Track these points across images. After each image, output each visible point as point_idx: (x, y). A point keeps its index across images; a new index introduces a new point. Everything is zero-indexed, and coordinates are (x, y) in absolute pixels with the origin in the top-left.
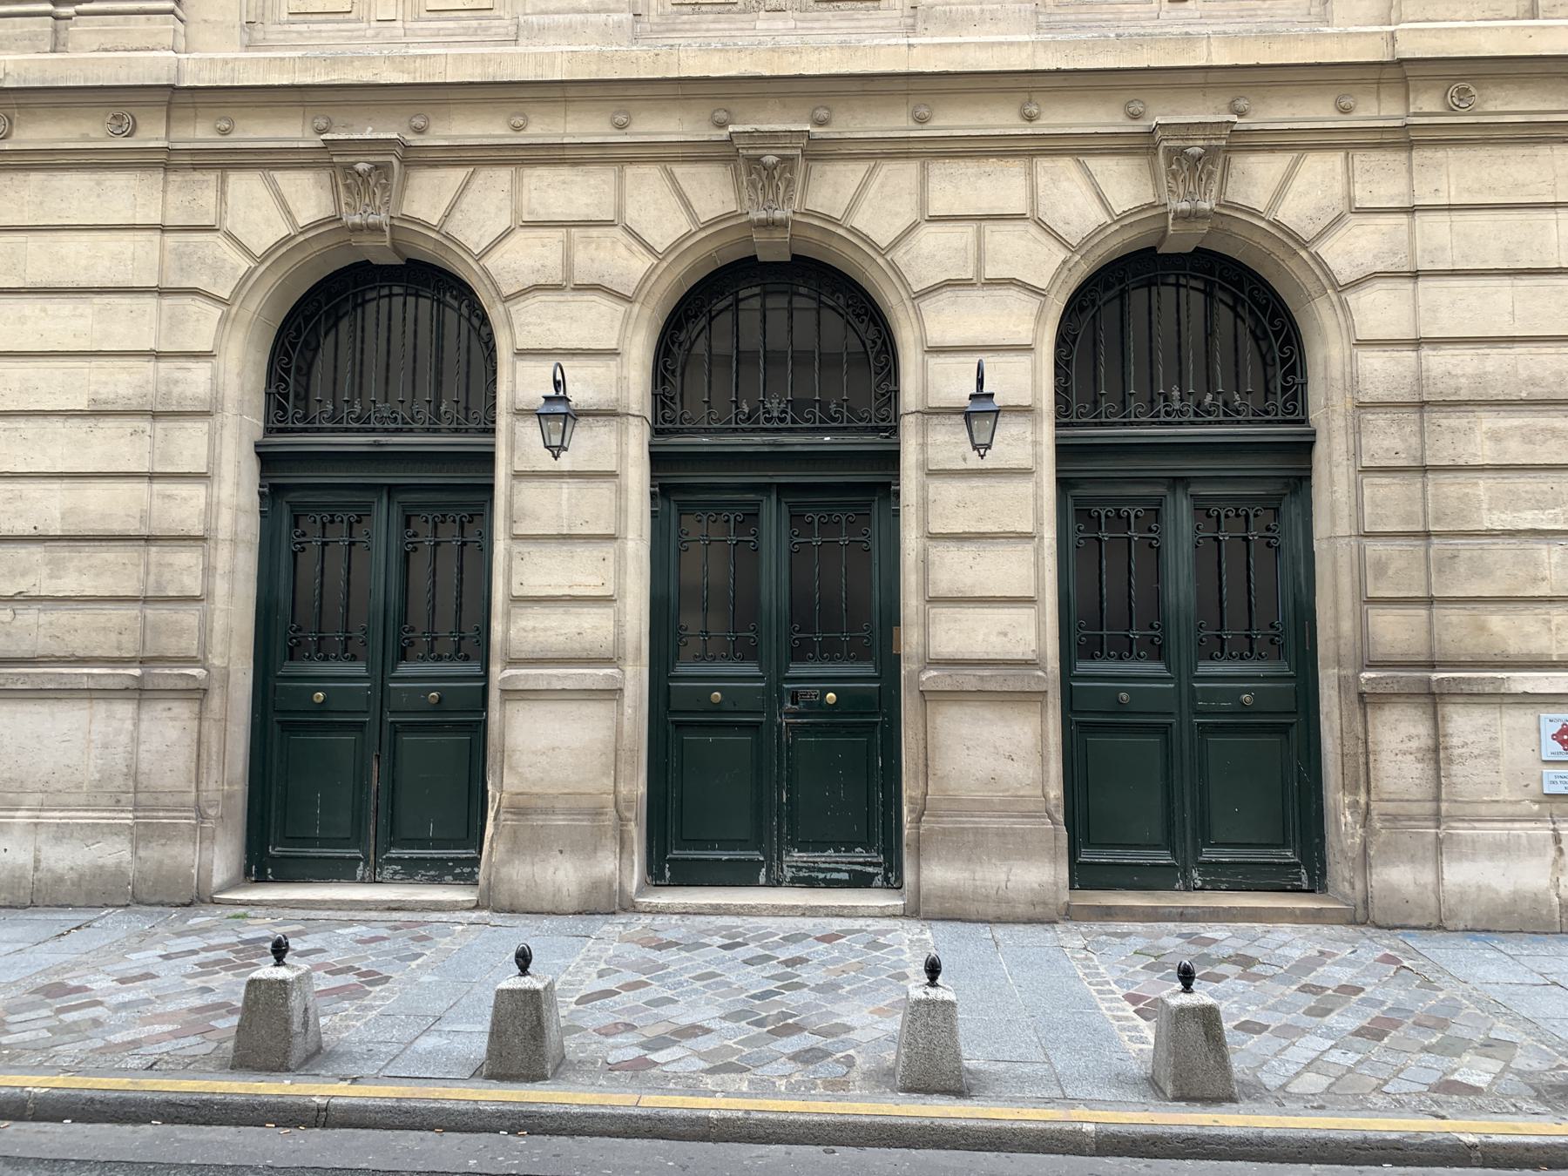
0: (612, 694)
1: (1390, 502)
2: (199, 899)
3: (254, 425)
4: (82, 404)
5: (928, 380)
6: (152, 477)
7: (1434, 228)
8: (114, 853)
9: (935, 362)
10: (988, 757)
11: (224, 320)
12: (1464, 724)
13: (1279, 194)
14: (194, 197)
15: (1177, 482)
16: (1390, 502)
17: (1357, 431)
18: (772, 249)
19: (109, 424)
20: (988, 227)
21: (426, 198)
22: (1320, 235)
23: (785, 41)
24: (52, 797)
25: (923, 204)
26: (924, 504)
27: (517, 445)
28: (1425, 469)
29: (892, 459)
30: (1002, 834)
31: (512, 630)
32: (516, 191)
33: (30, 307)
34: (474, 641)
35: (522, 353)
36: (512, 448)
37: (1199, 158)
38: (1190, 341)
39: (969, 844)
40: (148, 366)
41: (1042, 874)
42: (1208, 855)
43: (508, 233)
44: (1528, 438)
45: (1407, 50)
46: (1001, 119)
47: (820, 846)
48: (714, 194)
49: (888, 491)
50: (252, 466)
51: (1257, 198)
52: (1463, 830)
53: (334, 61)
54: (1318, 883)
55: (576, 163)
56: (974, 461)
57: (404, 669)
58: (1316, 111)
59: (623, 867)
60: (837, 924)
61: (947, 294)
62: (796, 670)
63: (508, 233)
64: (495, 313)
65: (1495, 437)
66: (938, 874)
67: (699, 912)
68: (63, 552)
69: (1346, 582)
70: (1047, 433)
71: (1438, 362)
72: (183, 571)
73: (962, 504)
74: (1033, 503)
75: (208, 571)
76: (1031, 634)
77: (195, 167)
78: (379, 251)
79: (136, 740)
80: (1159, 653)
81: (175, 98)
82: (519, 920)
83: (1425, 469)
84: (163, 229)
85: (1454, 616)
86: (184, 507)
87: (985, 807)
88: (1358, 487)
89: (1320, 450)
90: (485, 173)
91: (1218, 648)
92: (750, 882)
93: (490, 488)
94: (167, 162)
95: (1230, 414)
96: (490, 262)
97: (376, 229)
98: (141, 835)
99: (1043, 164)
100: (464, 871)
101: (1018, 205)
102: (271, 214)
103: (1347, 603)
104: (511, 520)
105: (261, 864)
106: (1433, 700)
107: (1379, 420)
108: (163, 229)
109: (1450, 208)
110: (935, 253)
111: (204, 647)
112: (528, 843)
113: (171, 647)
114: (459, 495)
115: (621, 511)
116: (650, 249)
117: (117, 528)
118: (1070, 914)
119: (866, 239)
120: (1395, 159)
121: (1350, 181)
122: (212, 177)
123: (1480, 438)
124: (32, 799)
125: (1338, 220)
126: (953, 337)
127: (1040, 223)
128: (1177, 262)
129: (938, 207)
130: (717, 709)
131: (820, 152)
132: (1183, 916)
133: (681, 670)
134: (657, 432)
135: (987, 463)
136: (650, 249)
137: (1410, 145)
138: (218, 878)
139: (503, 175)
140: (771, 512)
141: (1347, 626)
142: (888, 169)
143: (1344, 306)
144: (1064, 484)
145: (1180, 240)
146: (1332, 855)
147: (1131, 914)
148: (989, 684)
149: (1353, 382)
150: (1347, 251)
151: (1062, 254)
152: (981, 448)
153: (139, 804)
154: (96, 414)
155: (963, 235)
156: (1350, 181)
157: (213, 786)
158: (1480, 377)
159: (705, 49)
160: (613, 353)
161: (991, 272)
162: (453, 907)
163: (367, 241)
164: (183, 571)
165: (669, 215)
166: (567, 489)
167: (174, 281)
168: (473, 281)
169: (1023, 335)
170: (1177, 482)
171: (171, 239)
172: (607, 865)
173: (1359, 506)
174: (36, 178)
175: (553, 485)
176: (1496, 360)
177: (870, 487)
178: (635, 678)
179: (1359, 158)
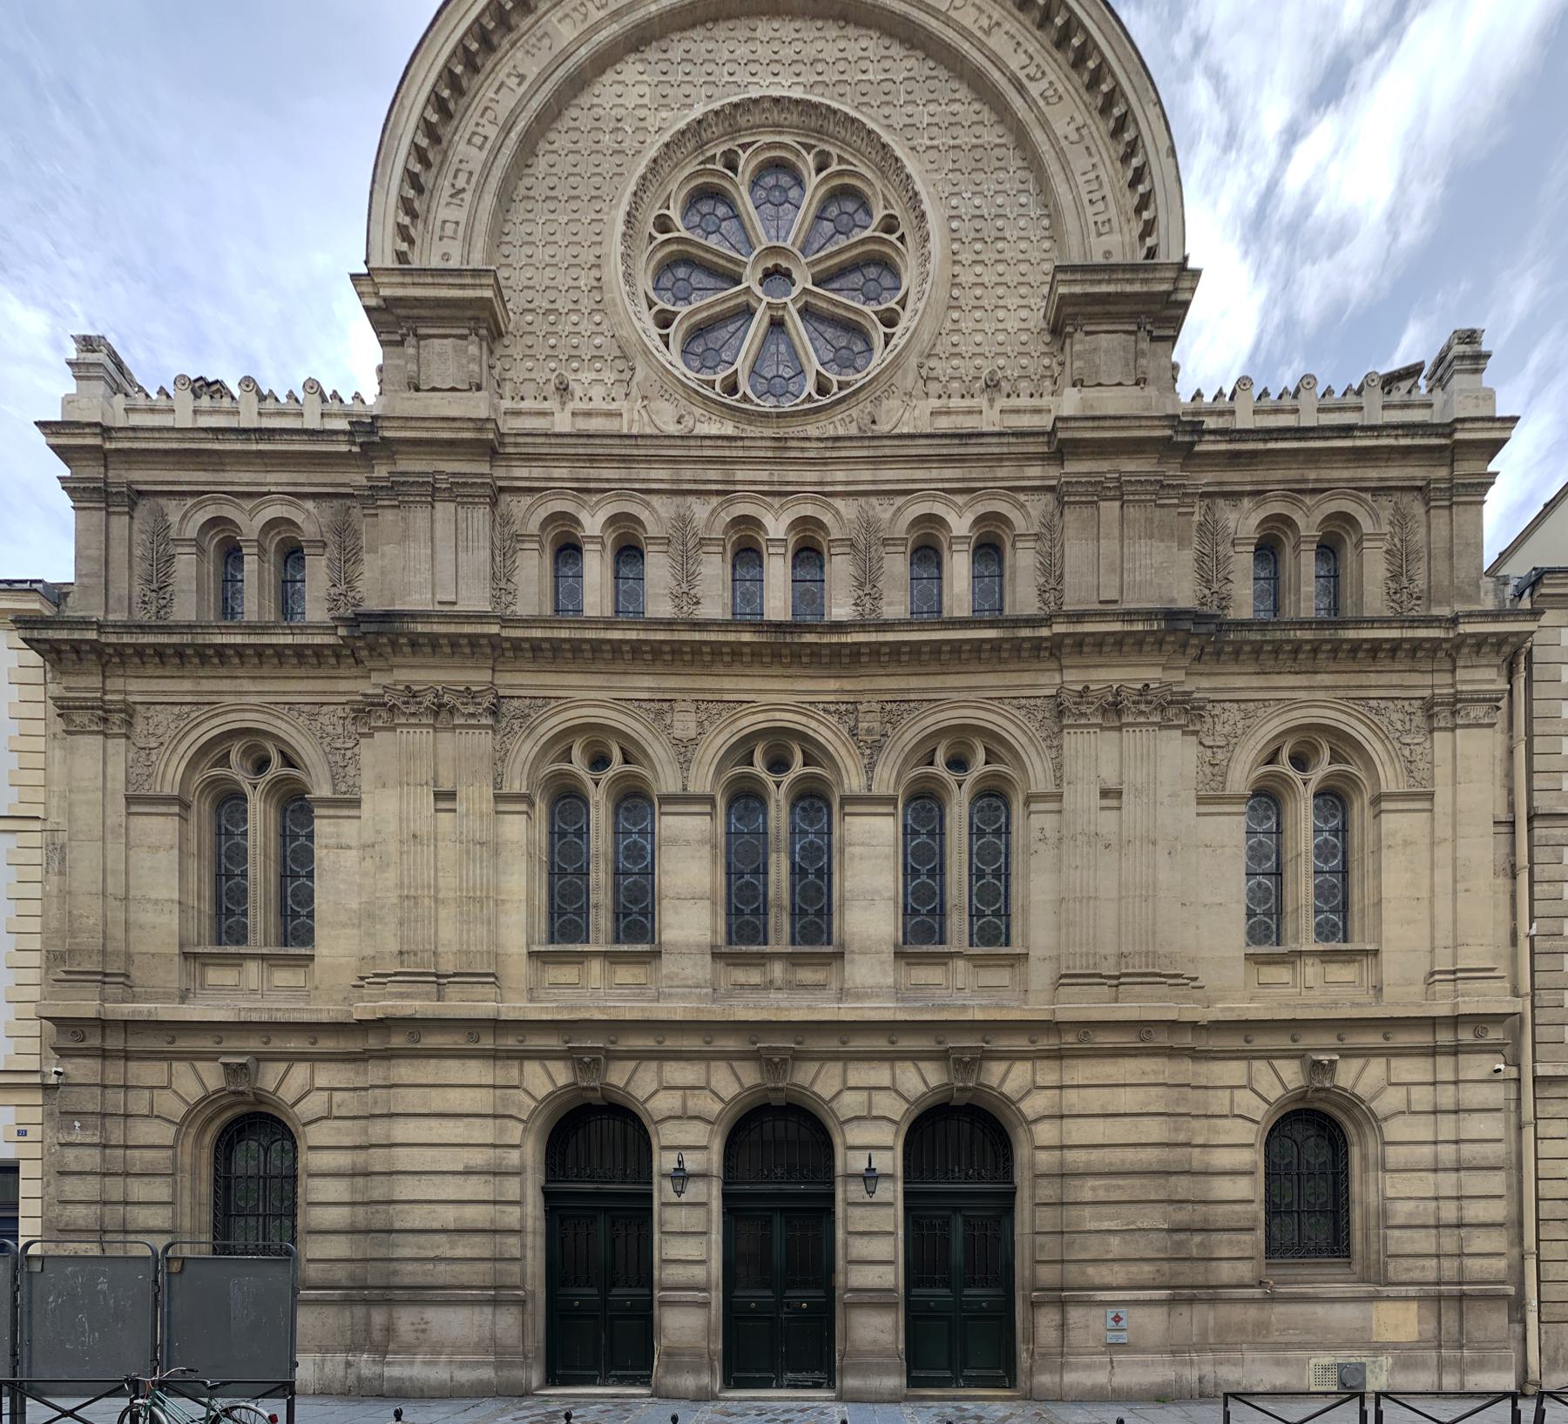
0: (706, 1304)
1: (1047, 1218)
2: (527, 1393)
3: (540, 1178)
4: (460, 1168)
5: (849, 1161)
6: (495, 1202)
7: (1072, 1096)
8: (487, 1374)
9: (851, 1154)
10: (875, 1332)
11: (525, 1130)
12: (1075, 1314)
13: (1003, 1080)
14: (509, 1072)
15: (956, 1209)
16: (1047, 1218)
17: (1034, 1188)
18: (777, 1100)
19: (474, 1178)
20: (874, 1093)
21: (617, 1075)
22: (1021, 1099)
23: (783, 1004)
24: (457, 1348)
25: (845, 1081)
26: (846, 1218)
27: (663, 1191)
28: (1062, 1204)
29: (832, 1196)
30: (878, 1364)
31: (664, 1274)
32: (660, 1071)
33: (434, 1122)
34: (644, 1277)
35: (664, 1148)
36: (660, 1191)
37: (969, 1062)
38: (962, 1144)
39: (864, 1370)
40: (491, 1151)
41: (895, 1382)
42: (967, 1372)
43: (656, 1092)
44: (1107, 1189)
45: (1060, 1017)
46: (880, 1044)
47: (800, 1371)
48: (750, 1075)
49: (830, 1212)
50: (540, 1199)
51: (993, 1081)
52: (1072, 1359)
53: (571, 1009)
54: (1012, 1385)
55: (687, 1059)
56: (867, 1199)
57: (615, 1291)
58: (1020, 1043)
59: (711, 1380)
60: (806, 1404)
61: (855, 1123)
62: (789, 1293)
63: (656, 1092)
64: (651, 1129)
65: (1093, 1189)
66: (851, 1382)
67: (746, 1400)
68: (456, 1237)
69: (1027, 1253)
70: (900, 1186)
71: (1071, 1156)
72: (512, 1245)
73: (862, 1218)
74: (893, 1219)
75: (523, 1246)
76: (891, 1277)
77: (508, 1058)
78: (595, 1098)
79: (494, 1323)
80: (947, 1285)
81: (497, 1025)
82: (671, 1402)
83: (1062, 1204)
84: (494, 1087)
85: (1073, 1268)
86: (511, 1216)
87: (872, 1353)
88: (1033, 1212)
89: (1018, 1196)
90: (645, 1064)
91: (972, 1283)
92: (770, 1387)
93: (651, 1209)
94: (494, 1056)
95: (980, 1179)
96: (648, 1106)
97: (594, 1089)
98: (498, 1366)
99: (899, 1064)
100: (644, 1381)
101: (887, 1082)
102: (543, 1081)
103: (1027, 1263)
104: (661, 1225)
105: (552, 1379)
106: (1062, 1304)
107: (1044, 1182)
108: (494, 1087)
109: (1078, 1086)
110: (851, 1103)
111: (523, 1280)
112: (674, 1367)
113: (509, 1281)
114: (635, 1214)
115: (709, 1221)
116: (722, 1100)
117: (480, 1226)
118: (907, 1399)
119: (819, 1097)
120: (1054, 1064)
121: (1034, 1074)
122: (516, 1063)
123: (1088, 1190)
124: (448, 1350)
125: (1028, 1092)
126: (858, 1141)
127: (896, 1091)
128: (958, 1109)
129: (851, 1083)
130: (752, 1311)
131: (799, 1057)
132: (955, 1399)
133: (737, 1293)
134: (725, 1183)
135: (874, 1200)
136: (722, 1100)
137: (1061, 1057)
138: (534, 1384)
139: (654, 1065)
140: (777, 1220)
141: (1027, 1273)
142: (829, 1065)
143: (1030, 1131)
144: (907, 1209)
145: (959, 1100)
146: (1019, 1372)
147: (932, 1398)
148: (875, 1300)
149: (1033, 1165)
150: (1033, 1105)
151: (906, 1106)
152: (871, 1193)
153: (495, 1348)
154: (468, 1173)
155: (862, 1096)
156: (1034, 1074)
157: (529, 1343)
158: (1088, 1162)
159: (746, 1007)
160: (705, 1148)
161: (874, 1113)
162: (641, 1396)
163: (590, 1094)
164: (512, 1245)
165: (729, 1084)
166: (684, 1211)
167: (501, 1111)
168: (641, 1115)
169: (889, 1141)
170: (956, 1209)
171: (498, 1092)
172: (705, 1380)
173: (1033, 1221)
174: (433, 1061)
175: (678, 1209)
176: (1095, 1155)
177: (822, 1210)
178: (716, 1297)
179: (1038, 1064)
